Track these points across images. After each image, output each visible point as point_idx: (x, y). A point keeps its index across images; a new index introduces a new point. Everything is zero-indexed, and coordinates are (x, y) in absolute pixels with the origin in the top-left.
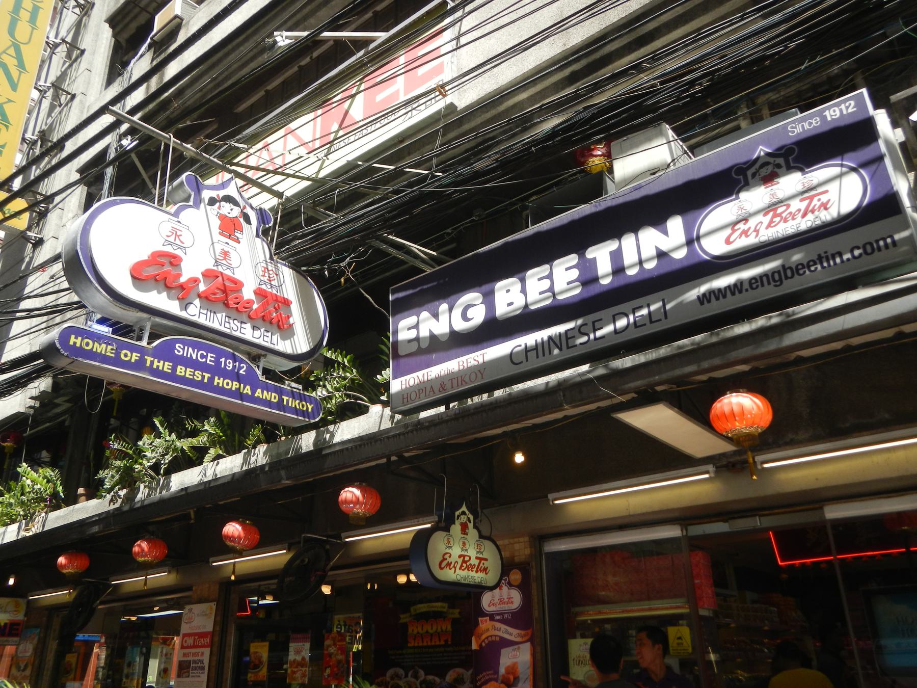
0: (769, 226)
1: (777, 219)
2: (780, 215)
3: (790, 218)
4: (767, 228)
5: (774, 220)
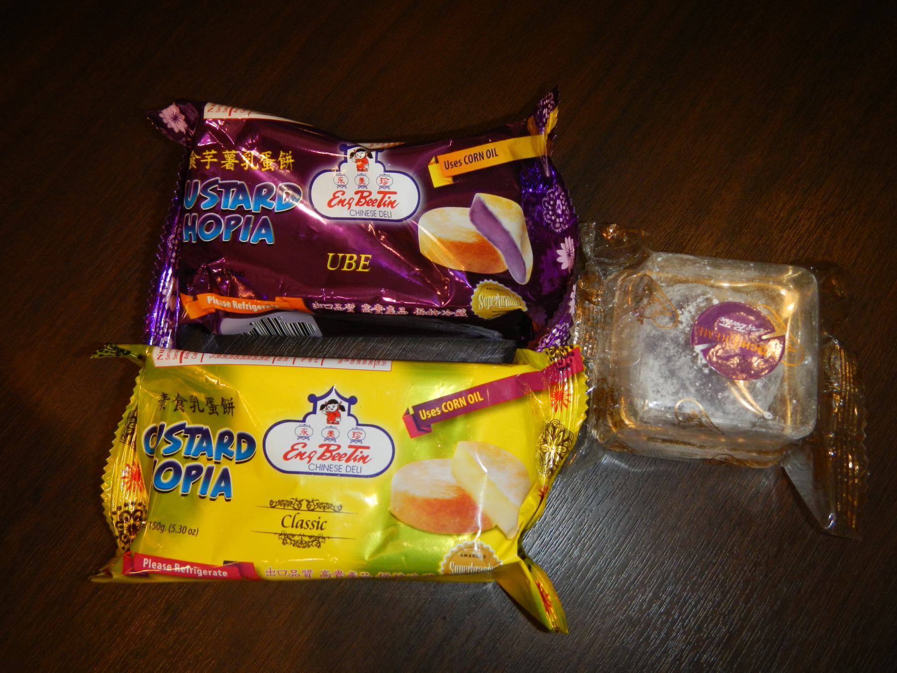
1: (328, 455)
2: (331, 452)
3: (338, 458)
4: (318, 459)
5: (326, 454)
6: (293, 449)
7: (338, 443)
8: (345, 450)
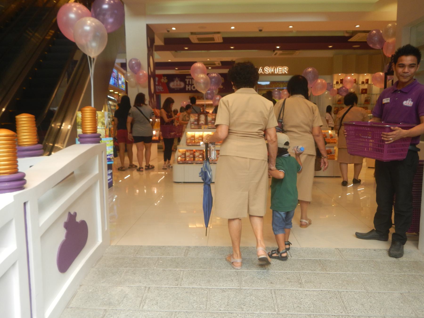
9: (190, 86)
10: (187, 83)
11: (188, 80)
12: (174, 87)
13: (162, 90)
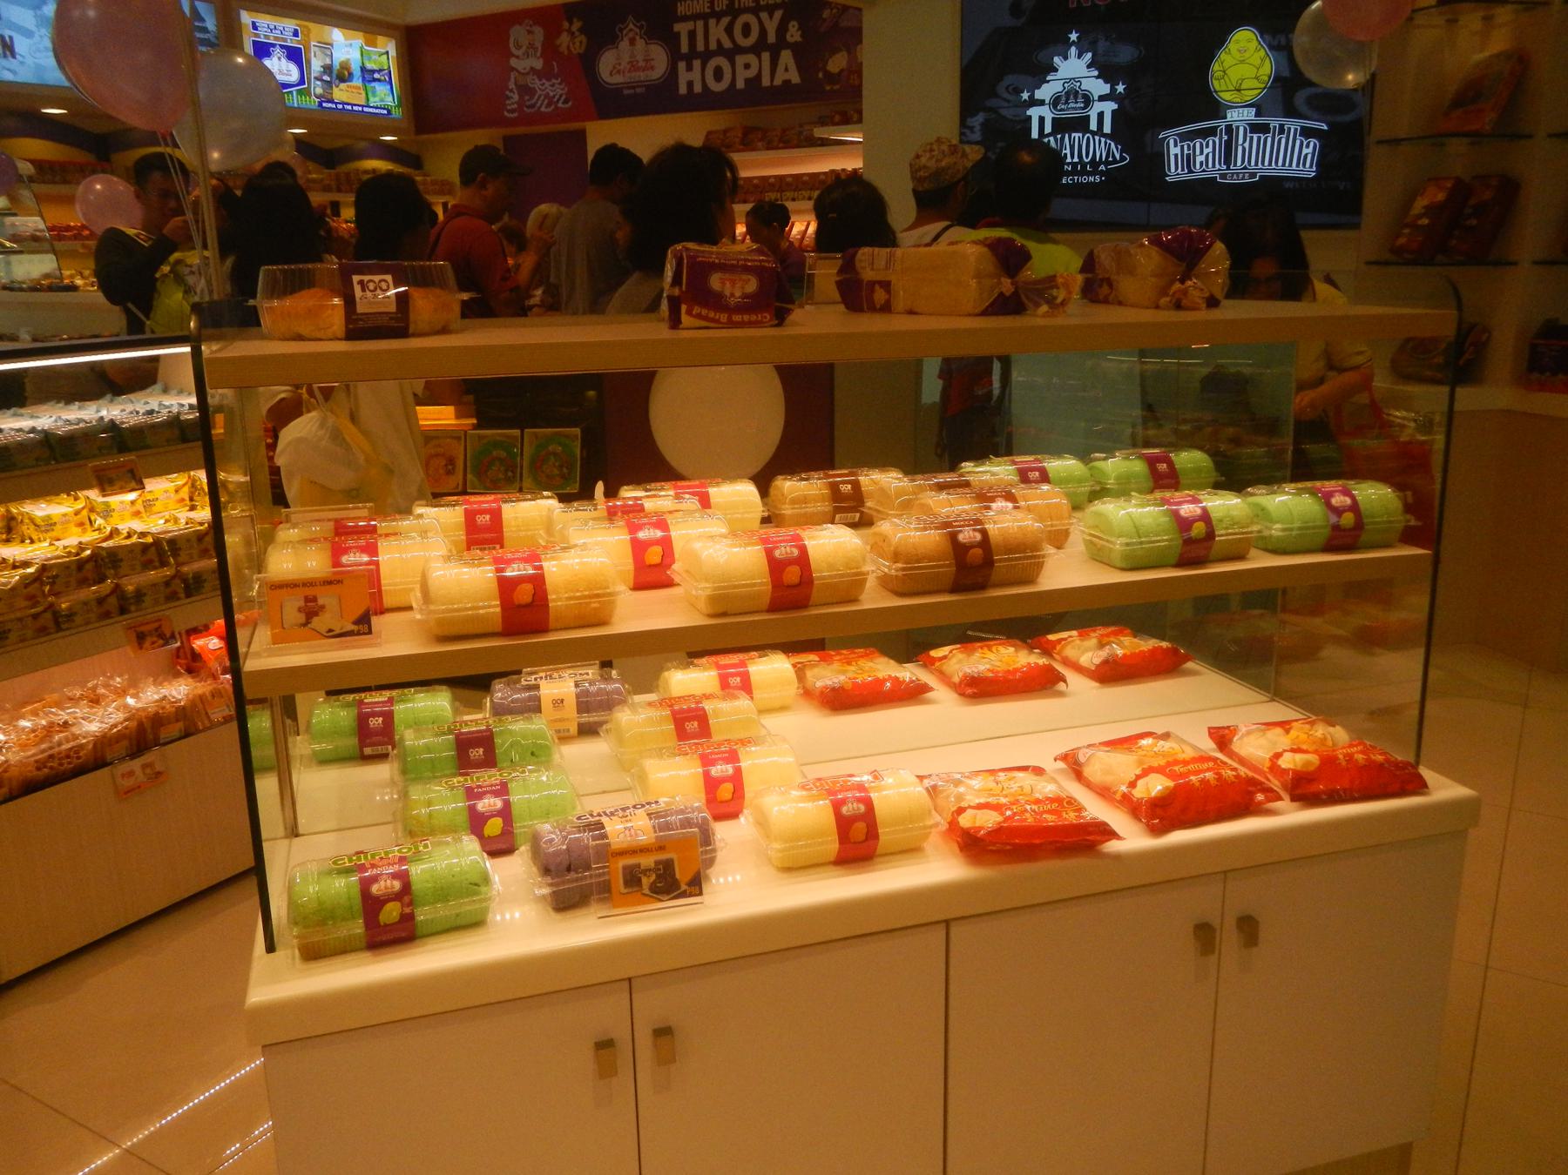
0: (629, 72)
6: (614, 68)
7: (637, 58)
8: (642, 64)
9: (697, 64)
10: (685, 48)
11: (689, 25)
12: (618, 79)
13: (566, 102)
